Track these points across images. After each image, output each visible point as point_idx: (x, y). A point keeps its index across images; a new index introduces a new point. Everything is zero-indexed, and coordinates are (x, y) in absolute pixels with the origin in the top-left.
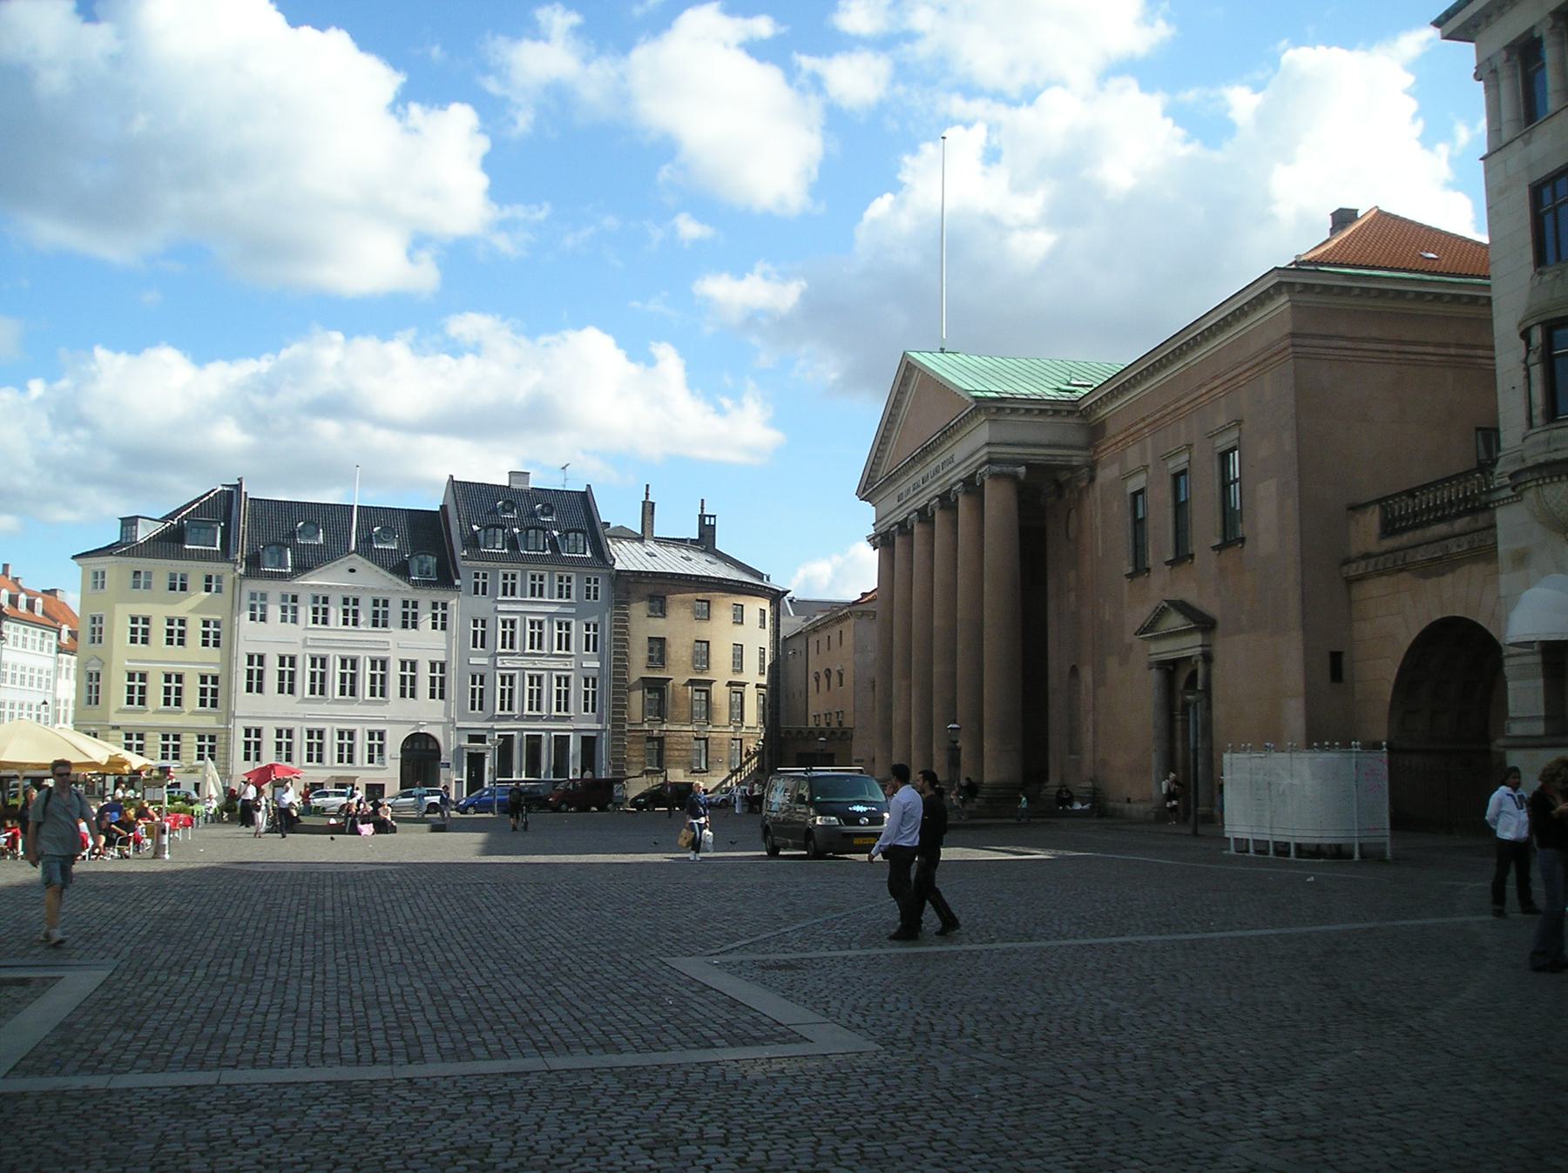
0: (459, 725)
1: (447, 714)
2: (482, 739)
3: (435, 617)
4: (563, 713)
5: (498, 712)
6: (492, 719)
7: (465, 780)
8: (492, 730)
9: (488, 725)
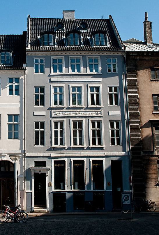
0: (28, 154)
1: (21, 148)
2: (44, 164)
3: (11, 87)
4: (97, 146)
5: (54, 146)
6: (50, 149)
7: (33, 191)
8: (50, 157)
9: (48, 154)
